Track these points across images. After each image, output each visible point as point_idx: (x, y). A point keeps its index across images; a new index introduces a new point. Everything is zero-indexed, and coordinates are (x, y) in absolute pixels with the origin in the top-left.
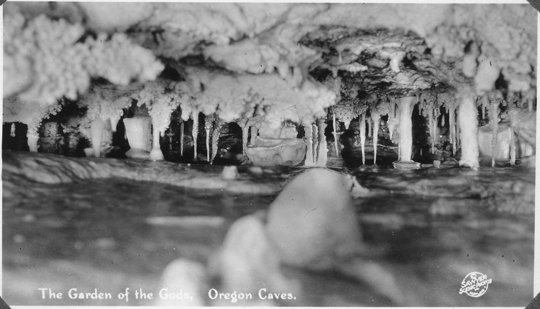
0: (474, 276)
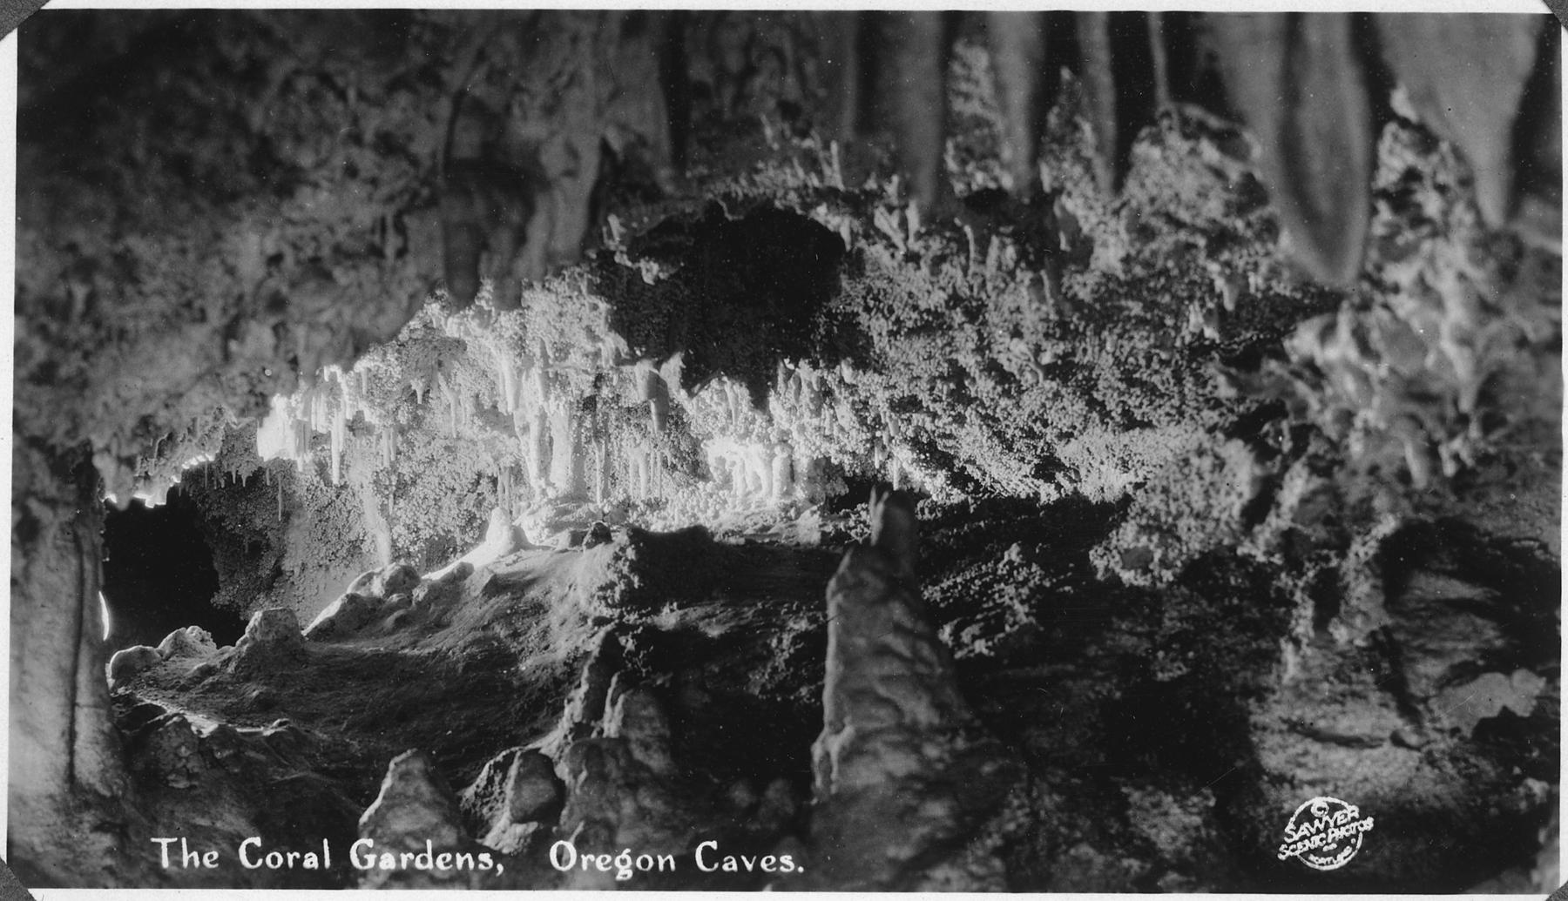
0: (1320, 809)
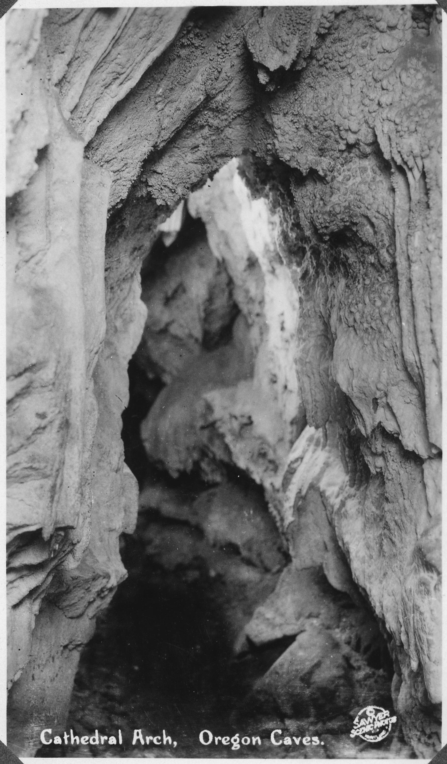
0: (371, 712)
